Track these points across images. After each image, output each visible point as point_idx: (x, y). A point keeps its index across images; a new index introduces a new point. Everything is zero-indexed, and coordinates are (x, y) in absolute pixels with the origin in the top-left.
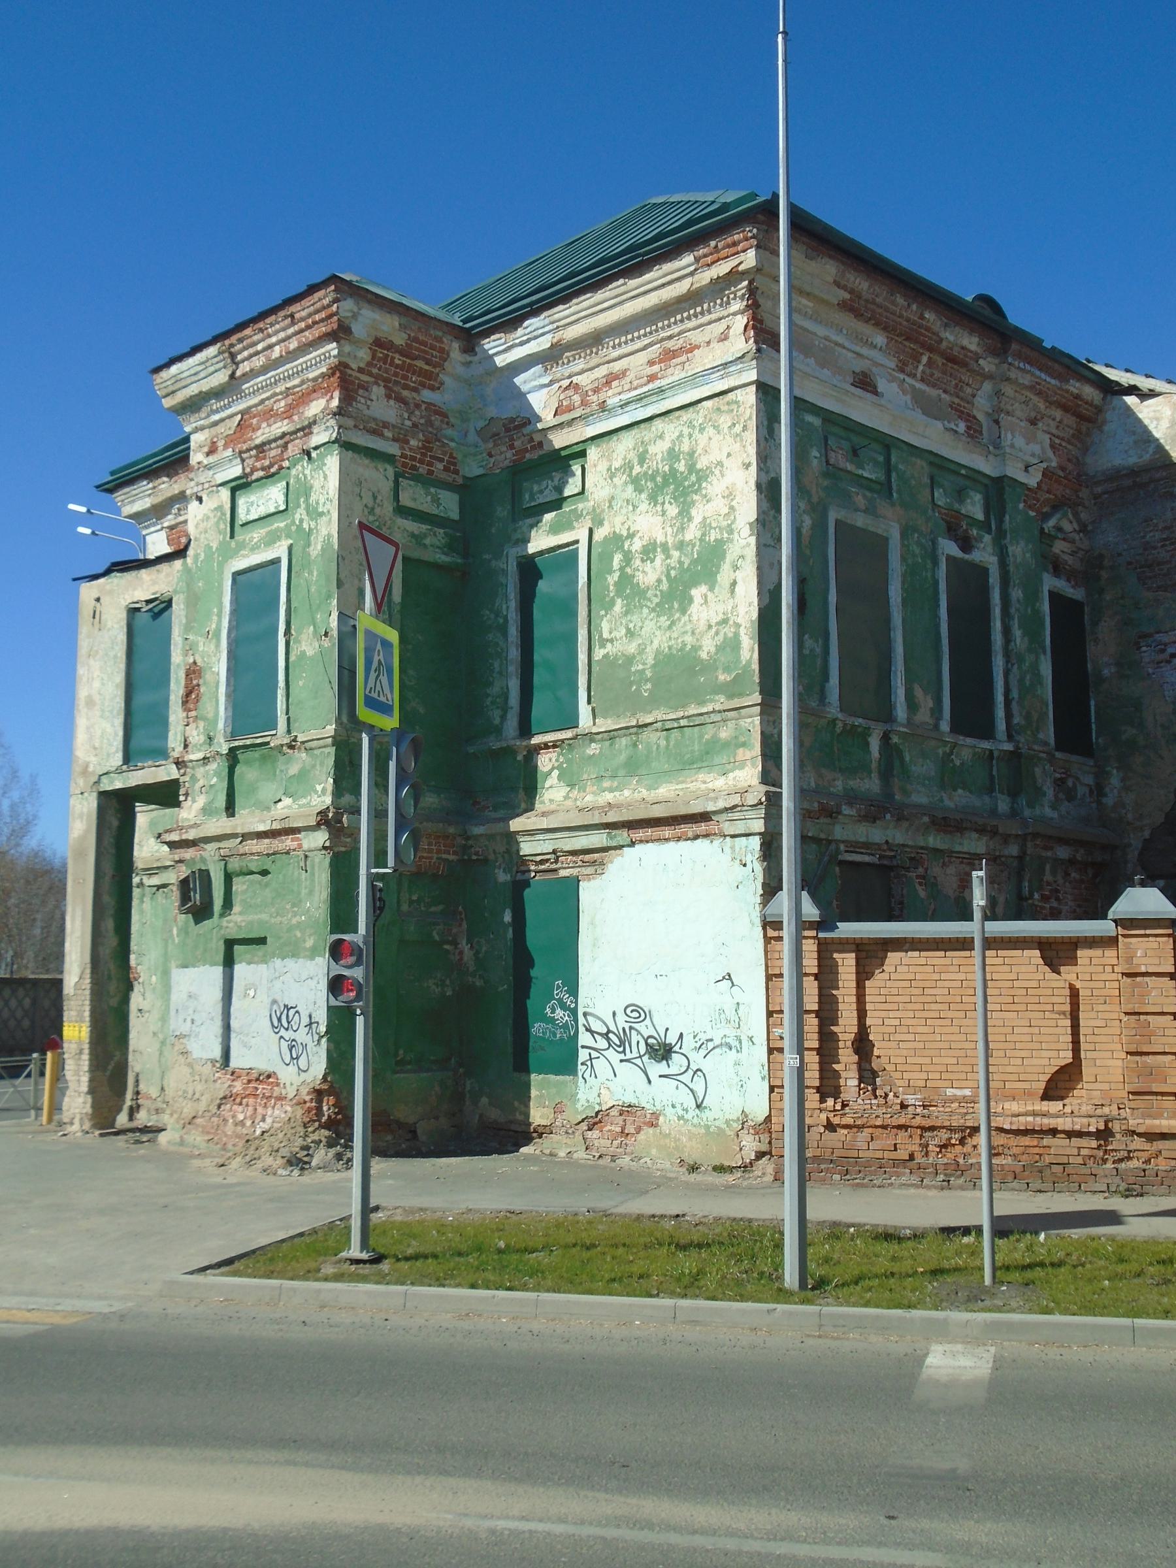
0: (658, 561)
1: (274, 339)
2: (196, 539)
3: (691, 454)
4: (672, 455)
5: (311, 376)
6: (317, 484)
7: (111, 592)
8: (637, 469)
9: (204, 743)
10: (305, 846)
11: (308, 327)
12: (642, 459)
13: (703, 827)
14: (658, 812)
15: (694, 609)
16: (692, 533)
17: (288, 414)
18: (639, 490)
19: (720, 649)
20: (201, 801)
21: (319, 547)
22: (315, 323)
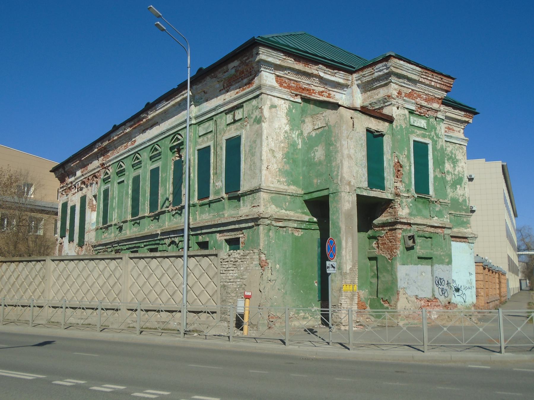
0: (450, 175)
1: (434, 80)
3: (455, 154)
4: (451, 152)
5: (436, 96)
6: (438, 128)
10: (445, 233)
11: (443, 85)
13: (465, 240)
14: (460, 235)
17: (426, 100)
22: (446, 85)
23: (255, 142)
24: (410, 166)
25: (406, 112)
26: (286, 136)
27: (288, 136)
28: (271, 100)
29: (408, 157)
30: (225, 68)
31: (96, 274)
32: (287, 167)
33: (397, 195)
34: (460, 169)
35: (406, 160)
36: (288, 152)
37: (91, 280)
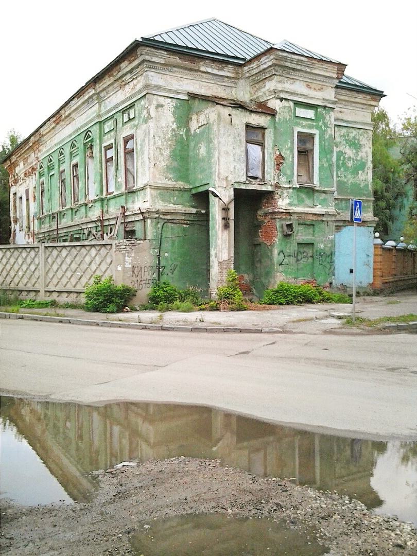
0: (351, 162)
2: (279, 113)
3: (359, 140)
4: (354, 138)
6: (327, 118)
7: (236, 115)
8: (347, 138)
9: (286, 182)
12: (348, 135)
15: (359, 176)
16: (359, 158)
18: (347, 143)
19: (364, 186)
20: (287, 201)
21: (328, 136)
23: (144, 140)
24: (293, 157)
25: (292, 104)
26: (173, 133)
27: (175, 134)
28: (157, 99)
29: (292, 150)
30: (118, 68)
31: (20, 261)
32: (175, 164)
33: (277, 186)
34: (364, 154)
35: (288, 152)
36: (175, 149)
37: (16, 267)
